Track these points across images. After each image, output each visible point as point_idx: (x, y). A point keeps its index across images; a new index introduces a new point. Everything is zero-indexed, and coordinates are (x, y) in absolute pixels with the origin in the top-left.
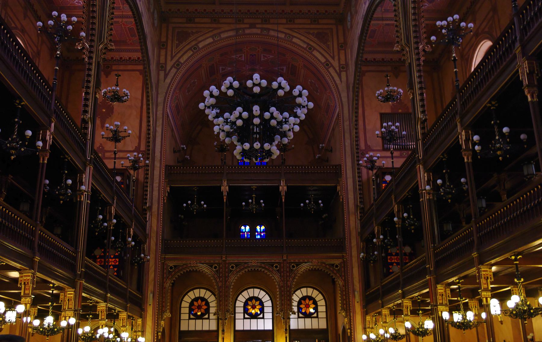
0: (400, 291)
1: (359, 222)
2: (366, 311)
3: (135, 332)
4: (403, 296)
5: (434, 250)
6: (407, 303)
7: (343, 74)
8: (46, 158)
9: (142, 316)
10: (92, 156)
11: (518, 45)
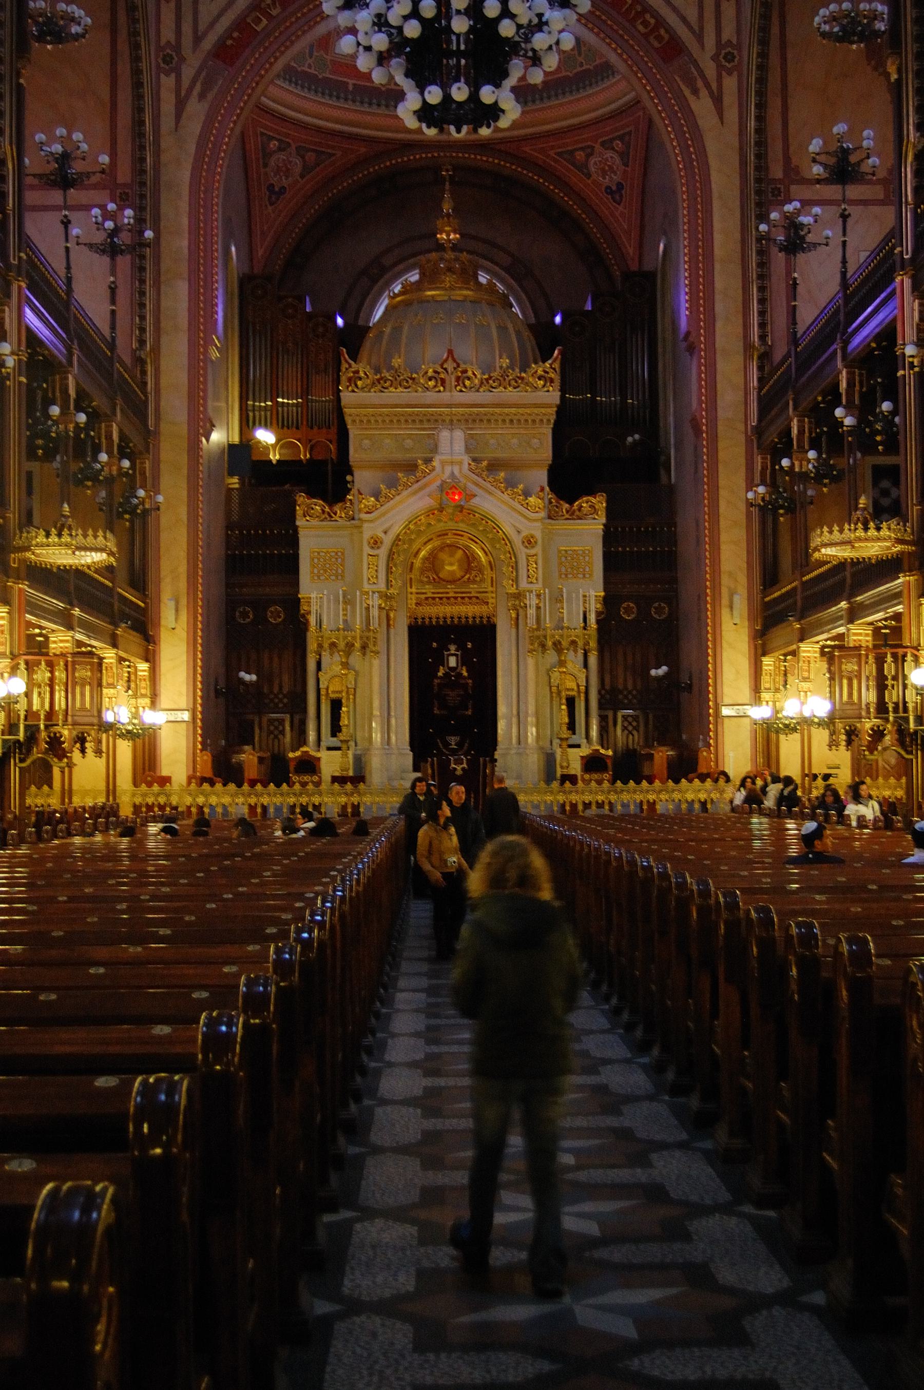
0: (843, 604)
1: (754, 396)
2: (764, 645)
3: (135, 696)
4: (852, 616)
6: (860, 634)
9: (150, 657)
10: (22, 255)
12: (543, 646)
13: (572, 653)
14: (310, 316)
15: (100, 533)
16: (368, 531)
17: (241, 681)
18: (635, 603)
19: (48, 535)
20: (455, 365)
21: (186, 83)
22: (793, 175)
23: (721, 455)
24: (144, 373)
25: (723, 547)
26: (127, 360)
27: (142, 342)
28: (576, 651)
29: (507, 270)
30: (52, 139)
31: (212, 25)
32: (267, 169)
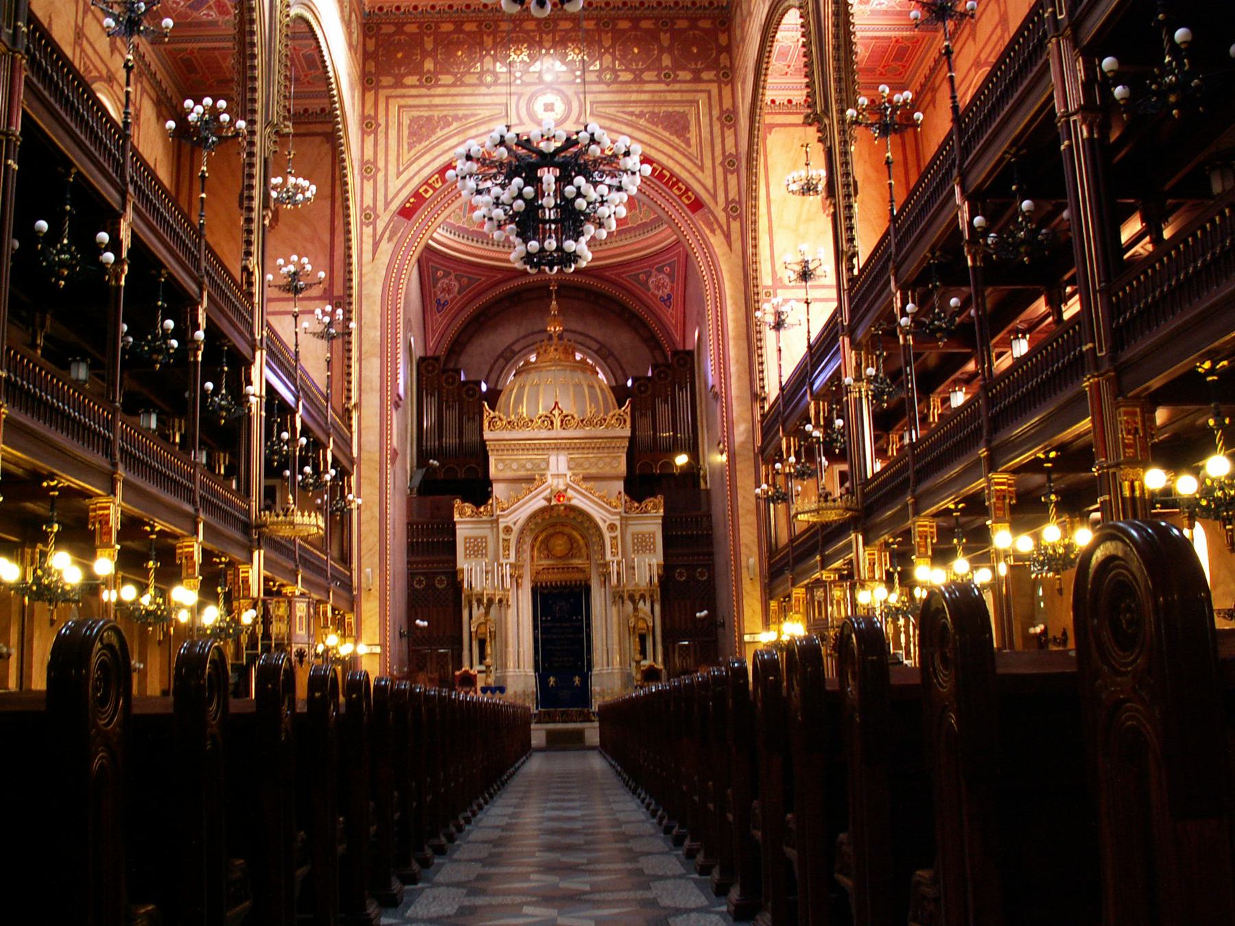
0: (818, 558)
1: (758, 427)
2: (771, 592)
5: (863, 490)
7: (729, 133)
8: (200, 353)
11: (955, 172)
12: (621, 597)
13: (641, 603)
14: (465, 383)
15: (313, 514)
16: (502, 523)
17: (417, 627)
19: (278, 516)
21: (379, 231)
22: (777, 283)
23: (738, 467)
24: (350, 418)
25: (741, 527)
26: (340, 410)
27: (349, 398)
28: (645, 602)
29: (596, 352)
30: (287, 262)
31: (396, 195)
32: (436, 289)
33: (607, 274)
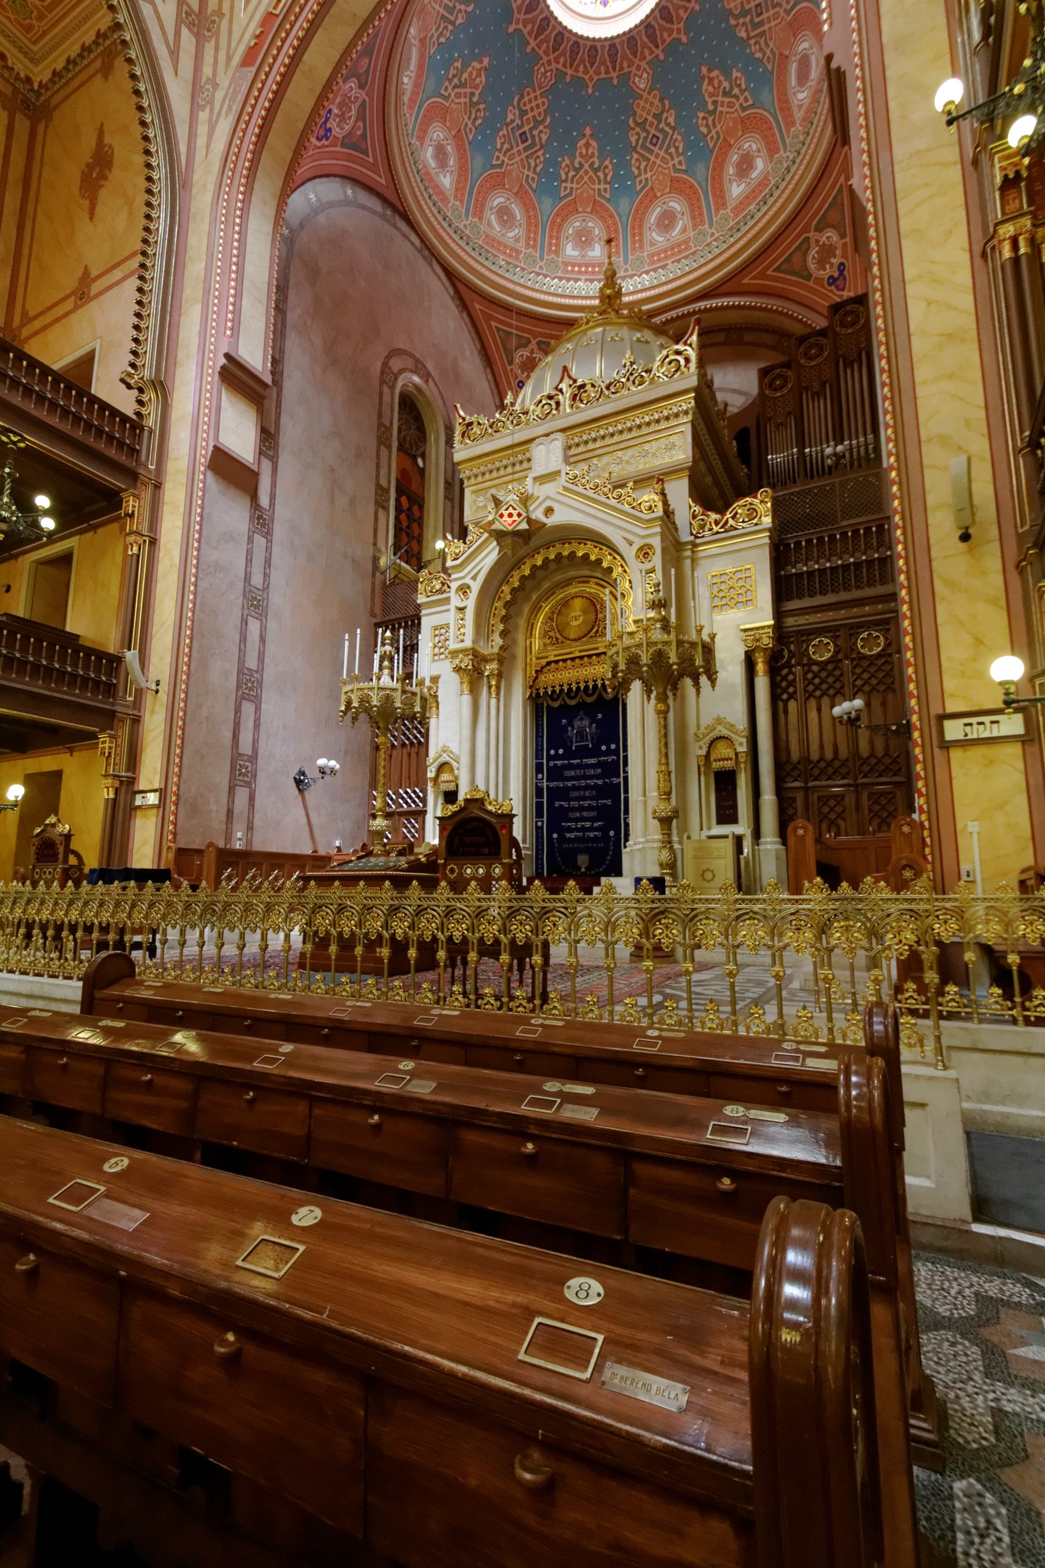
18: (830, 638)
20: (571, 382)
25: (920, 392)
33: (746, 281)
